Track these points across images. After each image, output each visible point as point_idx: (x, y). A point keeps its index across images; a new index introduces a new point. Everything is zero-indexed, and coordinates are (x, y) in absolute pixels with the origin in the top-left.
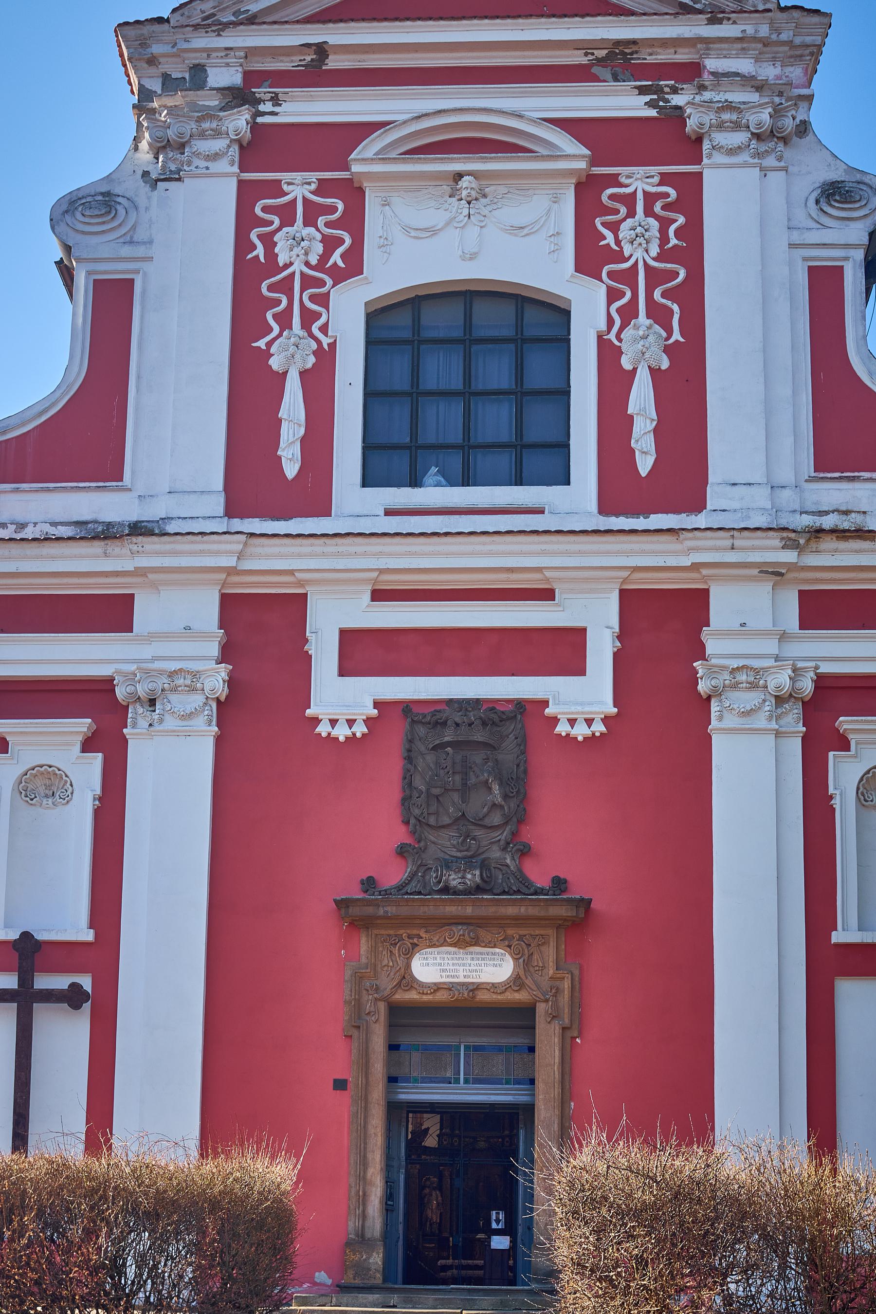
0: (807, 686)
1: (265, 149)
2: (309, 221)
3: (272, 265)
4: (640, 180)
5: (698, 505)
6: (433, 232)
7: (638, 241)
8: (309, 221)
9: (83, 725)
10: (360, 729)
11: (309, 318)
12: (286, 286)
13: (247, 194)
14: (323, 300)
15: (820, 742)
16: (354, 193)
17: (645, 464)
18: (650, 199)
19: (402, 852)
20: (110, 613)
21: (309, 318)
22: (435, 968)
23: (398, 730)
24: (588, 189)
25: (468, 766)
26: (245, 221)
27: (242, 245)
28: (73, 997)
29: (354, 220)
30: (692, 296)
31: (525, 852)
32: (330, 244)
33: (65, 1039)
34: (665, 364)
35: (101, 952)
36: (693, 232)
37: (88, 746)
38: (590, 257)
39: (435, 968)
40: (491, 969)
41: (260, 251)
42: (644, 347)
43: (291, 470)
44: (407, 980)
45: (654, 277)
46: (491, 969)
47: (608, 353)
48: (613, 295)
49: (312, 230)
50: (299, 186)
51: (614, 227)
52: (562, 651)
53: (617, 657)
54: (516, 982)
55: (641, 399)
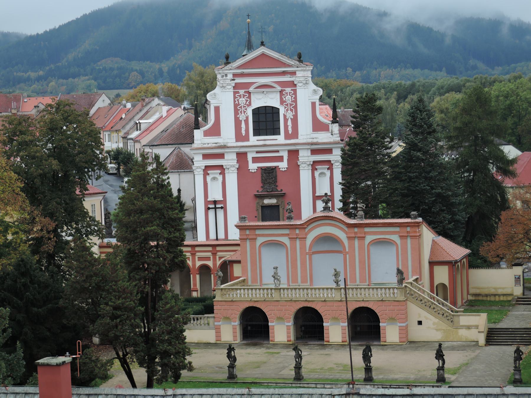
0: (312, 163)
1: (237, 87)
2: (244, 97)
3: (239, 104)
4: (288, 90)
5: (297, 138)
6: (260, 99)
7: (288, 99)
8: (244, 97)
9: (220, 171)
10: (255, 171)
11: (244, 112)
12: (241, 107)
13: (235, 93)
14: (246, 109)
15: (314, 169)
16: (250, 93)
17: (290, 132)
18: (290, 93)
19: (262, 187)
20: (221, 156)
21: (244, 112)
22: (267, 201)
23: (260, 171)
24: (281, 92)
25: (269, 175)
26: (235, 97)
27: (235, 101)
28: (222, 208)
29: (249, 97)
30: (296, 107)
31: (277, 186)
32: (247, 101)
33: (220, 213)
34: (292, 117)
35: (224, 201)
36: (296, 98)
37: (220, 174)
38: (282, 102)
39: (267, 201)
40: (273, 201)
41: (237, 102)
42: (290, 115)
43: (244, 135)
44: (263, 203)
45: (291, 105)
46: (273, 201)
47: (285, 116)
48: (285, 108)
49: (244, 99)
50: (242, 92)
51: (285, 97)
52: (281, 159)
53: (288, 159)
54: (277, 202)
55: (289, 123)
